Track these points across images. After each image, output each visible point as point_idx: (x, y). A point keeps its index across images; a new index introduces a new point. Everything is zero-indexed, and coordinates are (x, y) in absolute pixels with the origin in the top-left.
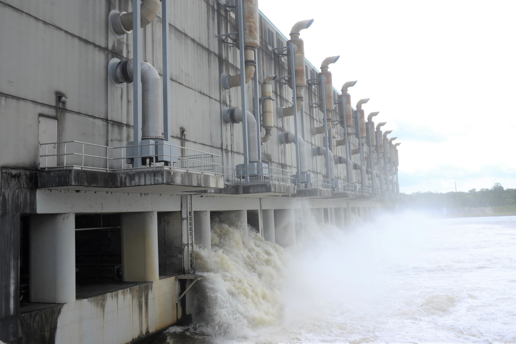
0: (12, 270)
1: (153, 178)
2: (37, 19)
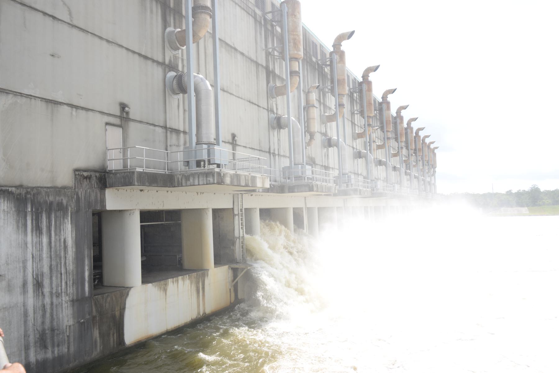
0: (86, 258)
2: (101, 38)
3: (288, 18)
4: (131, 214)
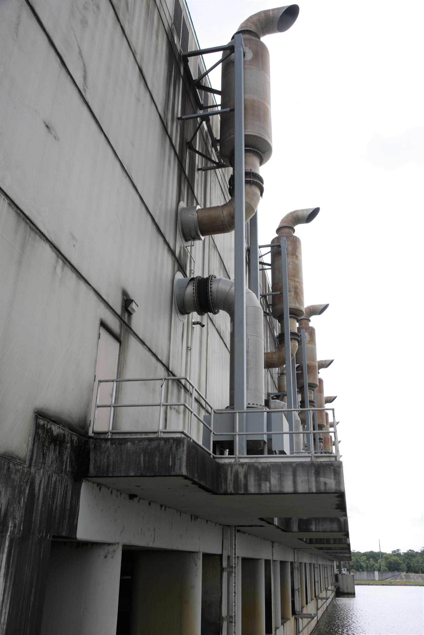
1: (313, 479)
4: (109, 556)
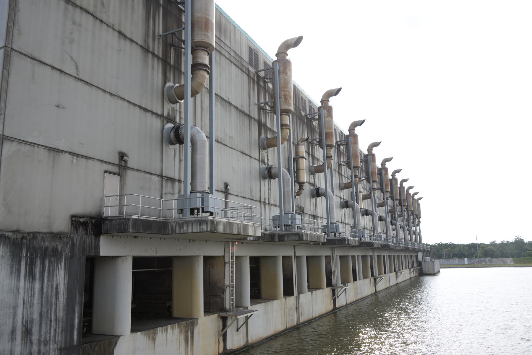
0: (77, 305)
1: (199, 226)
2: (104, 91)
3: (279, 76)
4: (124, 261)
